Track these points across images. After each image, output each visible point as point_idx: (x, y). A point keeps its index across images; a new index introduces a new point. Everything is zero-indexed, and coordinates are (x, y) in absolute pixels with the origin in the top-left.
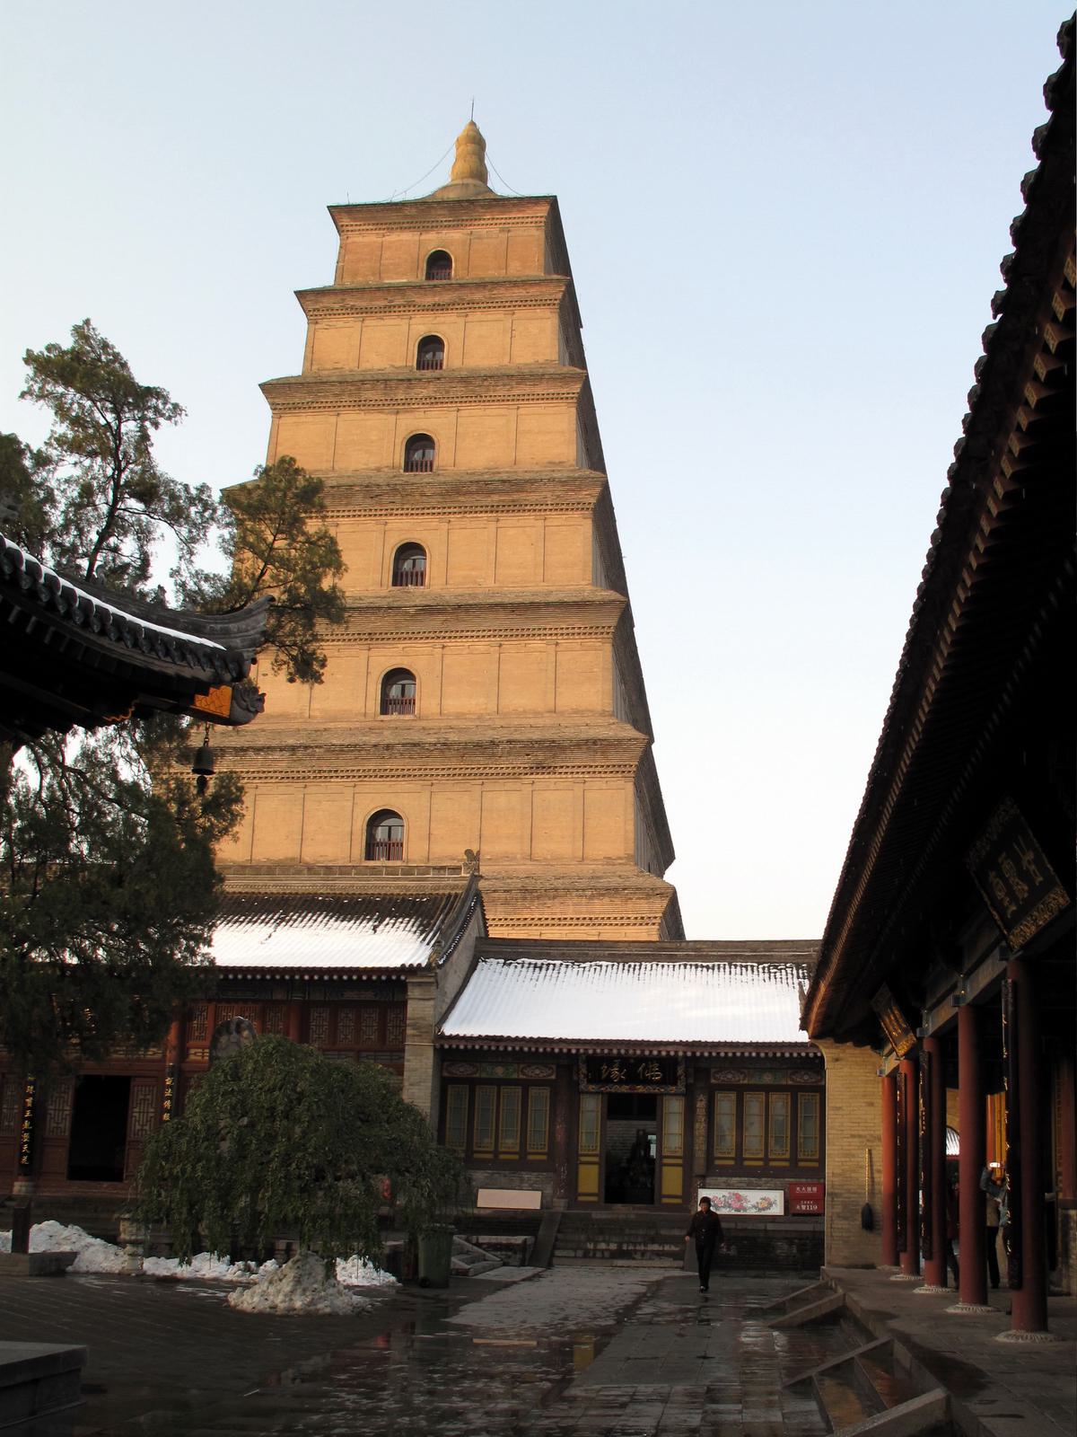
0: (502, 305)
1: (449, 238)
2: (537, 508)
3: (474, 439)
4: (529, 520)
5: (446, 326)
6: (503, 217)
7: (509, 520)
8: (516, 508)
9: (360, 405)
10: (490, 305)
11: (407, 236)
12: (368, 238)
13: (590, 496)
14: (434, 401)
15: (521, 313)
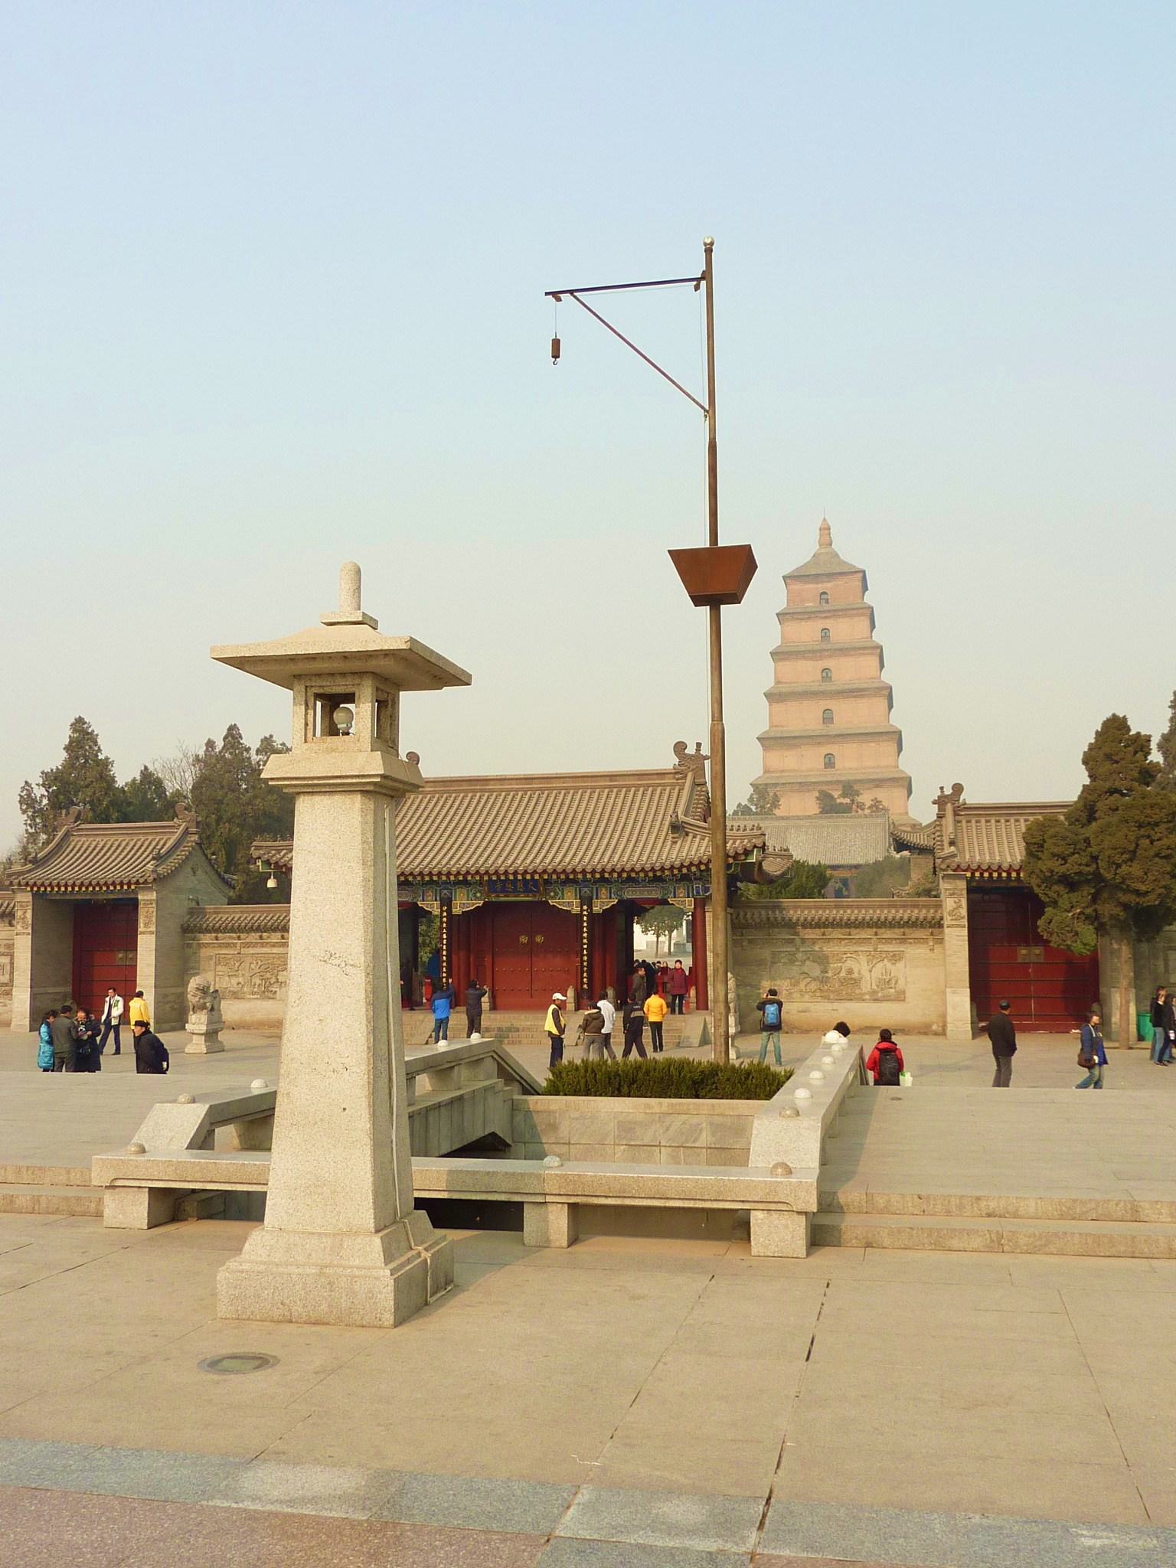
0: (851, 616)
1: (827, 586)
2: (868, 696)
3: (848, 671)
4: (865, 700)
5: (828, 623)
6: (845, 578)
7: (859, 700)
8: (862, 696)
9: (804, 658)
10: (845, 616)
11: (811, 586)
12: (797, 586)
13: (886, 692)
14: (830, 656)
15: (856, 619)
